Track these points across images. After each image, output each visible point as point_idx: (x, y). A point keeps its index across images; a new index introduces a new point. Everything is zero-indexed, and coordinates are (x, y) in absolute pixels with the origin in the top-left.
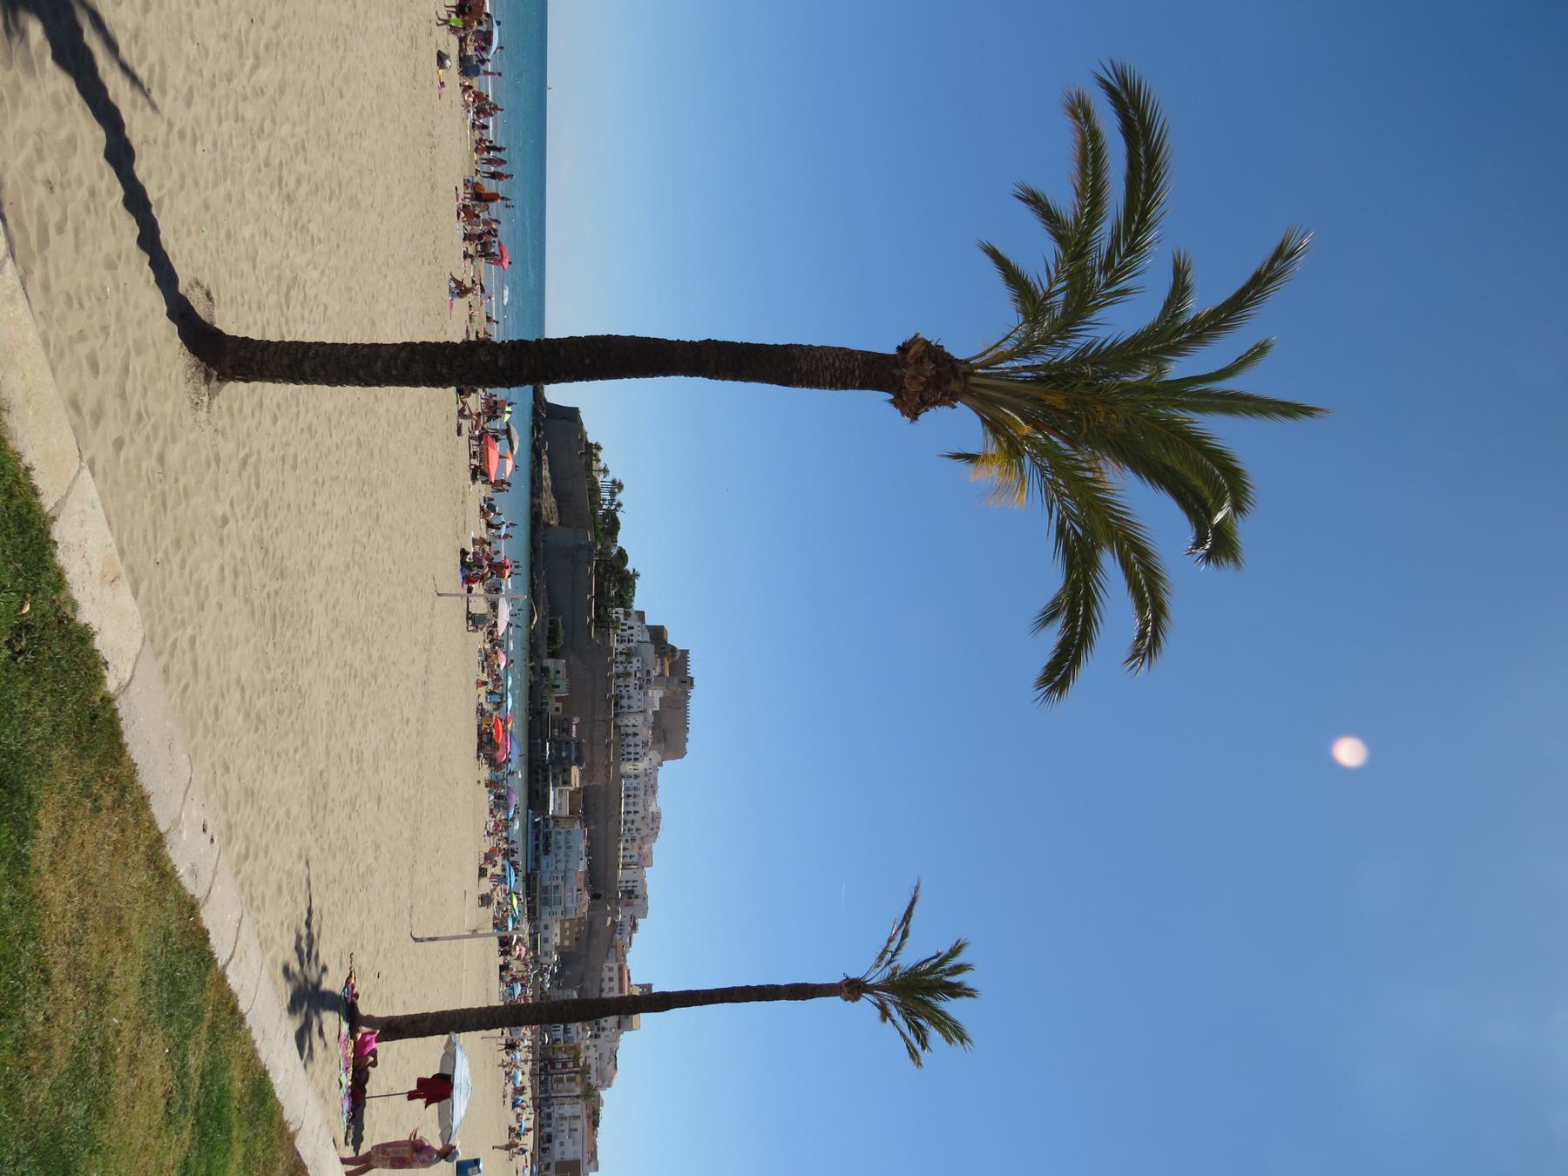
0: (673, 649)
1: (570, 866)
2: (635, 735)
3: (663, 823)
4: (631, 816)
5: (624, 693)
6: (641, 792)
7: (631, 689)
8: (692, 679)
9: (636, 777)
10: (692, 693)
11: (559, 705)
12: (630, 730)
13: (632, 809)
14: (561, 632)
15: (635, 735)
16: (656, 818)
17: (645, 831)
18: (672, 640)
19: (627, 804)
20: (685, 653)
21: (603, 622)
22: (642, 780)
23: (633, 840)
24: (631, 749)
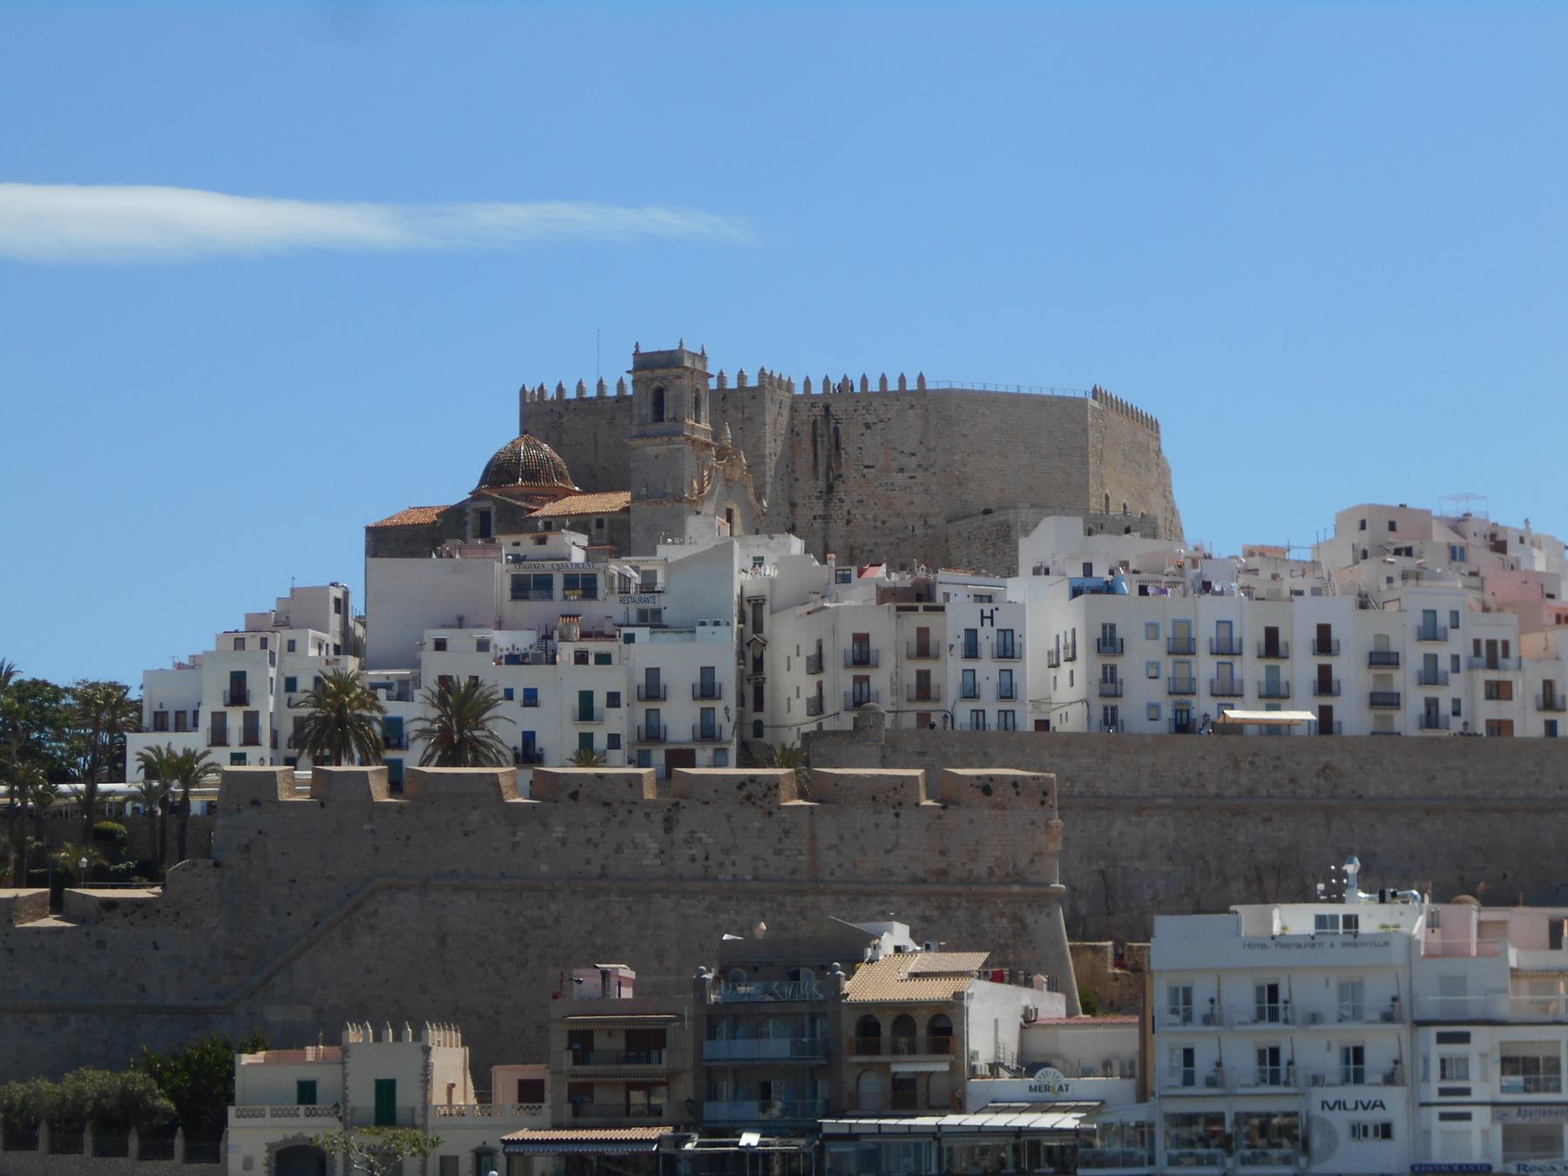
0: (499, 472)
1: (1377, 991)
2: (862, 654)
3: (1431, 490)
4: (1349, 669)
5: (616, 721)
6: (1205, 617)
7: (601, 681)
8: (645, 363)
9: (1109, 642)
10: (731, 359)
11: (506, 1079)
12: (839, 681)
13: (1301, 667)
14: (94, 1081)
15: (862, 654)
16: (1390, 536)
17: (1447, 591)
18: (454, 482)
19: (1274, 695)
20: (540, 413)
21: (155, 839)
22: (1126, 612)
23: (1492, 654)
24: (949, 672)
